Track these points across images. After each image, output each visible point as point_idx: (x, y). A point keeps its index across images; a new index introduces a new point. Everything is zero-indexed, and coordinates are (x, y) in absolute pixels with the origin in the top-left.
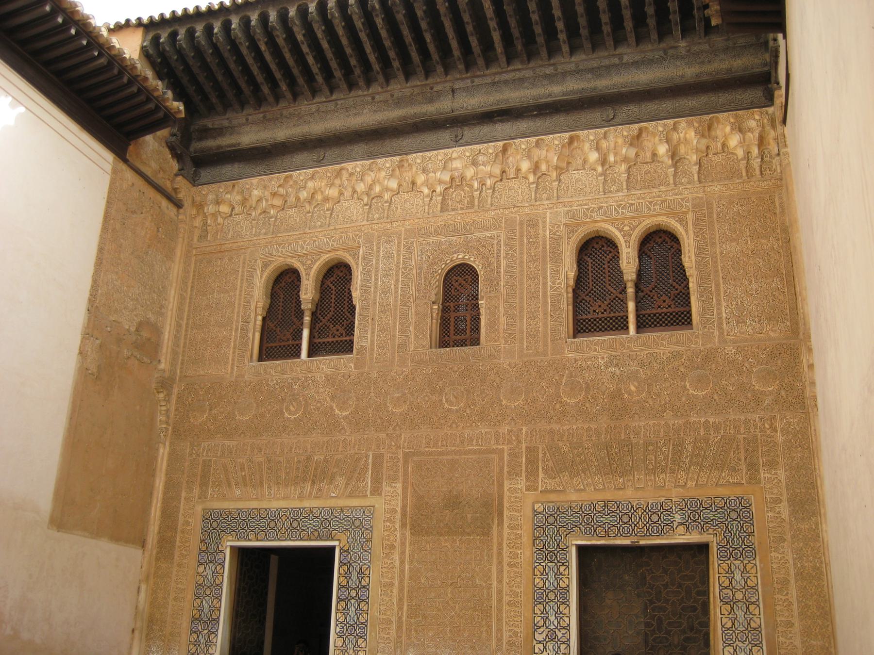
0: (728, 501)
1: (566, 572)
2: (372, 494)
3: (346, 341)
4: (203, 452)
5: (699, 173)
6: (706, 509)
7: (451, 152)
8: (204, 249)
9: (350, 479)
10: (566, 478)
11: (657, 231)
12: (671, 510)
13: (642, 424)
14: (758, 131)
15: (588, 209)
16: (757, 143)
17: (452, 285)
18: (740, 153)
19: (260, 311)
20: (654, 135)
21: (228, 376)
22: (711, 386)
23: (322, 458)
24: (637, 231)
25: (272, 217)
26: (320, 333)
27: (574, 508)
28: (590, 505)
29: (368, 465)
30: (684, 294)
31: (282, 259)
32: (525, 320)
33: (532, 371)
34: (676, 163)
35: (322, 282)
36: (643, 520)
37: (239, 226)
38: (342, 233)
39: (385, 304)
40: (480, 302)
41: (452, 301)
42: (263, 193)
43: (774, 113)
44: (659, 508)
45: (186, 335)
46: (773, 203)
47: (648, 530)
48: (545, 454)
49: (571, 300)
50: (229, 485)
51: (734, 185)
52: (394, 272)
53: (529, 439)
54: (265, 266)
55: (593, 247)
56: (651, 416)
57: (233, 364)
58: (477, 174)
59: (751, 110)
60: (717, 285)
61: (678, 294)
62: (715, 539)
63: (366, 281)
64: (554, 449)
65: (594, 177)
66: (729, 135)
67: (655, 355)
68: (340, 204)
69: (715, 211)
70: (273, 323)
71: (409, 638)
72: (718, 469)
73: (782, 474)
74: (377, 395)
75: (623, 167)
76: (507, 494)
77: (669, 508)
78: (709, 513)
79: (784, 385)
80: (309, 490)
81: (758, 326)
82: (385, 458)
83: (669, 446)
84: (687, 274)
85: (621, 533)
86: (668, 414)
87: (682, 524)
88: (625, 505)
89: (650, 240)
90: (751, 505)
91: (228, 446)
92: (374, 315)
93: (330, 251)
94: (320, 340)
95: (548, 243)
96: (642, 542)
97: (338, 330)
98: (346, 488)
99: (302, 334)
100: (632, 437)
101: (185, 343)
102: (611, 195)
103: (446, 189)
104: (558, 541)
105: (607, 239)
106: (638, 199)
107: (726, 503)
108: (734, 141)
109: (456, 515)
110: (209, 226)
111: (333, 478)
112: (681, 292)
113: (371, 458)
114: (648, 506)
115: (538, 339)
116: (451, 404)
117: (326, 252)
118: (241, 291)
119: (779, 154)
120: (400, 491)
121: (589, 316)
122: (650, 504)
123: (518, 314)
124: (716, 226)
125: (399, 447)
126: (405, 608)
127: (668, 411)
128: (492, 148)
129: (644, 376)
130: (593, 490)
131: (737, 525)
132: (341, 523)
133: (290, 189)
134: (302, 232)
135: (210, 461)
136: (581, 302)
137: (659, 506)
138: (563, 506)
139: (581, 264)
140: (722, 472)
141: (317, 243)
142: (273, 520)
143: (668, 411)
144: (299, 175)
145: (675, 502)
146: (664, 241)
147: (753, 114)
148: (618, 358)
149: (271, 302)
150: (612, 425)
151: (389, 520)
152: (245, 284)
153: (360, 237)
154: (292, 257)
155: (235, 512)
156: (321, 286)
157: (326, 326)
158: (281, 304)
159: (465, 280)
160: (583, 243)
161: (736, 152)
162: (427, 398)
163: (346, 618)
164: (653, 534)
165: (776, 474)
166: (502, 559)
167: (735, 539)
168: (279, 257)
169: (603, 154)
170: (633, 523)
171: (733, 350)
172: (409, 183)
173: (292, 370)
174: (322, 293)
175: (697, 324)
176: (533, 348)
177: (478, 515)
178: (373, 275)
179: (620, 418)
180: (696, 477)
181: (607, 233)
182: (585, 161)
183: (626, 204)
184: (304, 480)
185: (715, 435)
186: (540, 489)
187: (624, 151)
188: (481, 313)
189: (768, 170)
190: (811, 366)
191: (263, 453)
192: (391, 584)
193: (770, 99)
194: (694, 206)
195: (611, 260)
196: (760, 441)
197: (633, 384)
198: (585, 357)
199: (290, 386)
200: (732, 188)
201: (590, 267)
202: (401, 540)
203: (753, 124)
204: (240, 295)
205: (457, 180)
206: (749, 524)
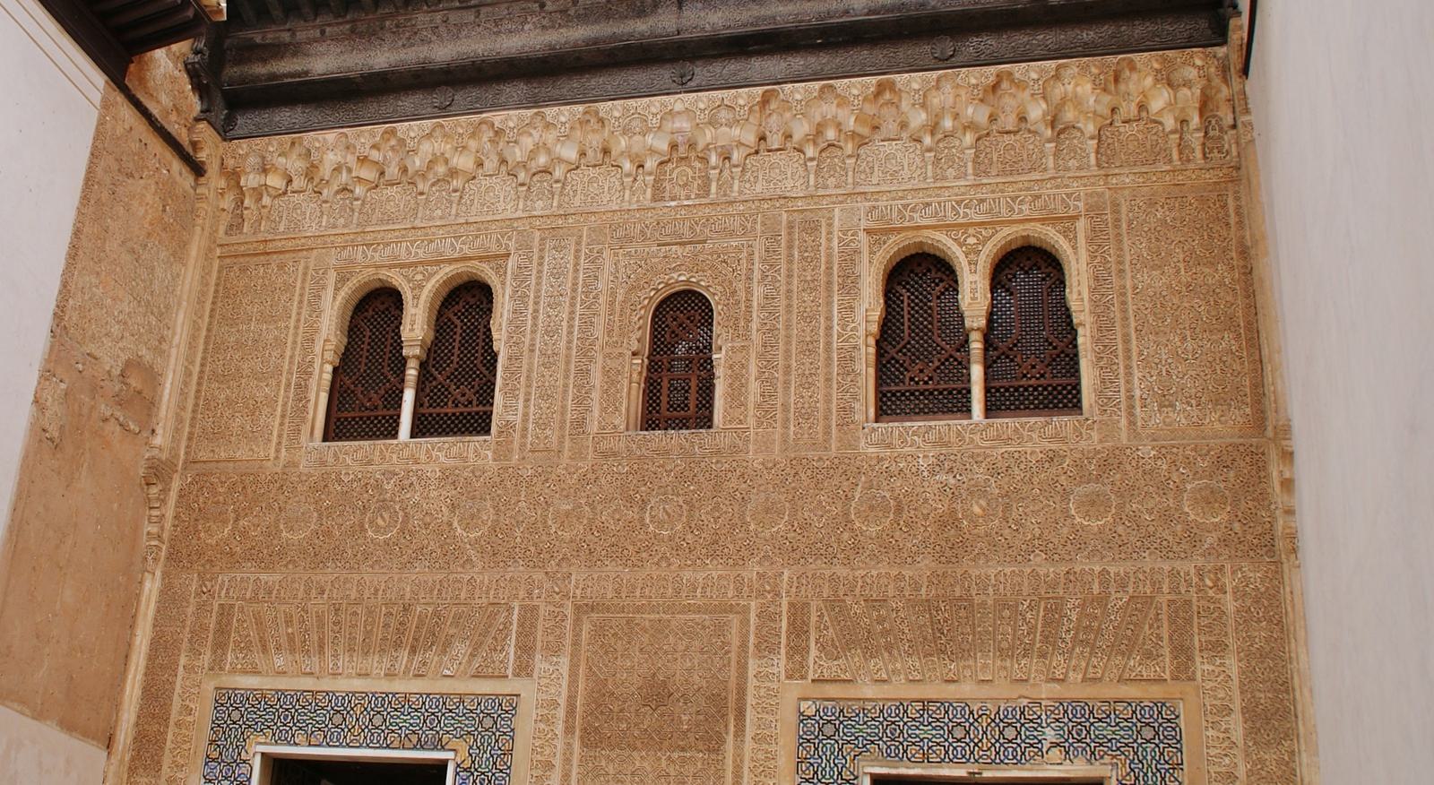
0: (1139, 708)
3: (477, 413)
5: (1097, 152)
6: (1100, 720)
7: (672, 101)
10: (856, 659)
11: (1023, 247)
12: (1039, 721)
13: (992, 572)
14: (1199, 86)
15: (905, 206)
16: (1197, 105)
17: (667, 326)
18: (1170, 122)
19: (329, 356)
20: (1020, 85)
22: (1114, 511)
24: (989, 245)
25: (357, 199)
26: (431, 398)
27: (869, 711)
28: (898, 708)
30: (1067, 355)
32: (793, 389)
33: (802, 475)
34: (1059, 134)
35: (439, 312)
36: (989, 737)
37: (299, 211)
38: (479, 230)
39: (549, 352)
40: (714, 356)
41: (665, 353)
42: (345, 158)
43: (1227, 56)
44: (1018, 717)
46: (1224, 206)
47: (998, 753)
49: (873, 357)
51: (1159, 175)
52: (567, 299)
53: (794, 589)
54: (342, 280)
55: (912, 271)
56: (1008, 559)
58: (716, 138)
59: (1188, 50)
60: (1127, 341)
61: (1058, 356)
62: (1114, 773)
64: (837, 609)
65: (918, 152)
66: (1150, 89)
67: (1016, 455)
68: (476, 181)
69: (1124, 216)
70: (350, 378)
72: (1123, 654)
73: (1233, 665)
74: (532, 506)
75: (969, 138)
76: (752, 682)
77: (1035, 716)
78: (1105, 729)
79: (1239, 514)
80: (404, 662)
83: (1039, 611)
84: (1075, 321)
85: (951, 757)
86: (1038, 559)
87: (1058, 745)
88: (959, 709)
89: (1011, 262)
90: (1177, 717)
92: (530, 371)
93: (456, 260)
94: (431, 410)
95: (836, 260)
96: (986, 774)
97: (463, 395)
99: (401, 398)
100: (974, 594)
102: (946, 184)
103: (661, 163)
104: (840, 766)
105: (935, 257)
106: (993, 192)
107: (1134, 712)
108: (1159, 101)
110: (246, 208)
112: (1062, 352)
114: (998, 713)
115: (815, 422)
116: (660, 525)
117: (451, 261)
118: (298, 321)
119: (1234, 127)
121: (902, 388)
122: (1002, 709)
123: (781, 378)
124: (1126, 243)
125: (566, 596)
127: (1037, 551)
128: (744, 96)
129: (997, 491)
130: (903, 681)
131: (1153, 750)
132: (460, 722)
133: (390, 153)
136: (889, 362)
137: (1019, 713)
138: (849, 707)
139: (890, 299)
140: (1128, 659)
141: (433, 246)
142: (339, 712)
143: (1037, 551)
145: (1046, 706)
146: (1035, 265)
147: (1192, 57)
148: (952, 457)
149: (349, 343)
150: (939, 572)
153: (510, 239)
154: (390, 267)
155: (273, 696)
156: (437, 320)
157: (443, 387)
158: (365, 347)
159: (688, 318)
160: (894, 264)
161: (1161, 119)
162: (617, 517)
164: (1006, 761)
165: (1222, 664)
167: (1150, 774)
168: (368, 267)
169: (934, 113)
170: (972, 740)
171: (1153, 453)
172: (598, 150)
174: (438, 331)
175: (1091, 406)
176: (806, 436)
177: (701, 717)
178: (531, 302)
179: (954, 560)
180: (1084, 664)
181: (939, 249)
182: (904, 125)
183: (971, 200)
185: (1118, 595)
186: (811, 676)
187: (970, 110)
188: (717, 374)
189: (1216, 151)
190: (1288, 484)
193: (1219, 35)
194: (1089, 208)
195: (943, 294)
196: (1195, 608)
197: (977, 502)
198: (896, 455)
200: (1155, 179)
201: (906, 304)
203: (1192, 73)
204: (296, 328)
205: (681, 149)
206: (1175, 750)
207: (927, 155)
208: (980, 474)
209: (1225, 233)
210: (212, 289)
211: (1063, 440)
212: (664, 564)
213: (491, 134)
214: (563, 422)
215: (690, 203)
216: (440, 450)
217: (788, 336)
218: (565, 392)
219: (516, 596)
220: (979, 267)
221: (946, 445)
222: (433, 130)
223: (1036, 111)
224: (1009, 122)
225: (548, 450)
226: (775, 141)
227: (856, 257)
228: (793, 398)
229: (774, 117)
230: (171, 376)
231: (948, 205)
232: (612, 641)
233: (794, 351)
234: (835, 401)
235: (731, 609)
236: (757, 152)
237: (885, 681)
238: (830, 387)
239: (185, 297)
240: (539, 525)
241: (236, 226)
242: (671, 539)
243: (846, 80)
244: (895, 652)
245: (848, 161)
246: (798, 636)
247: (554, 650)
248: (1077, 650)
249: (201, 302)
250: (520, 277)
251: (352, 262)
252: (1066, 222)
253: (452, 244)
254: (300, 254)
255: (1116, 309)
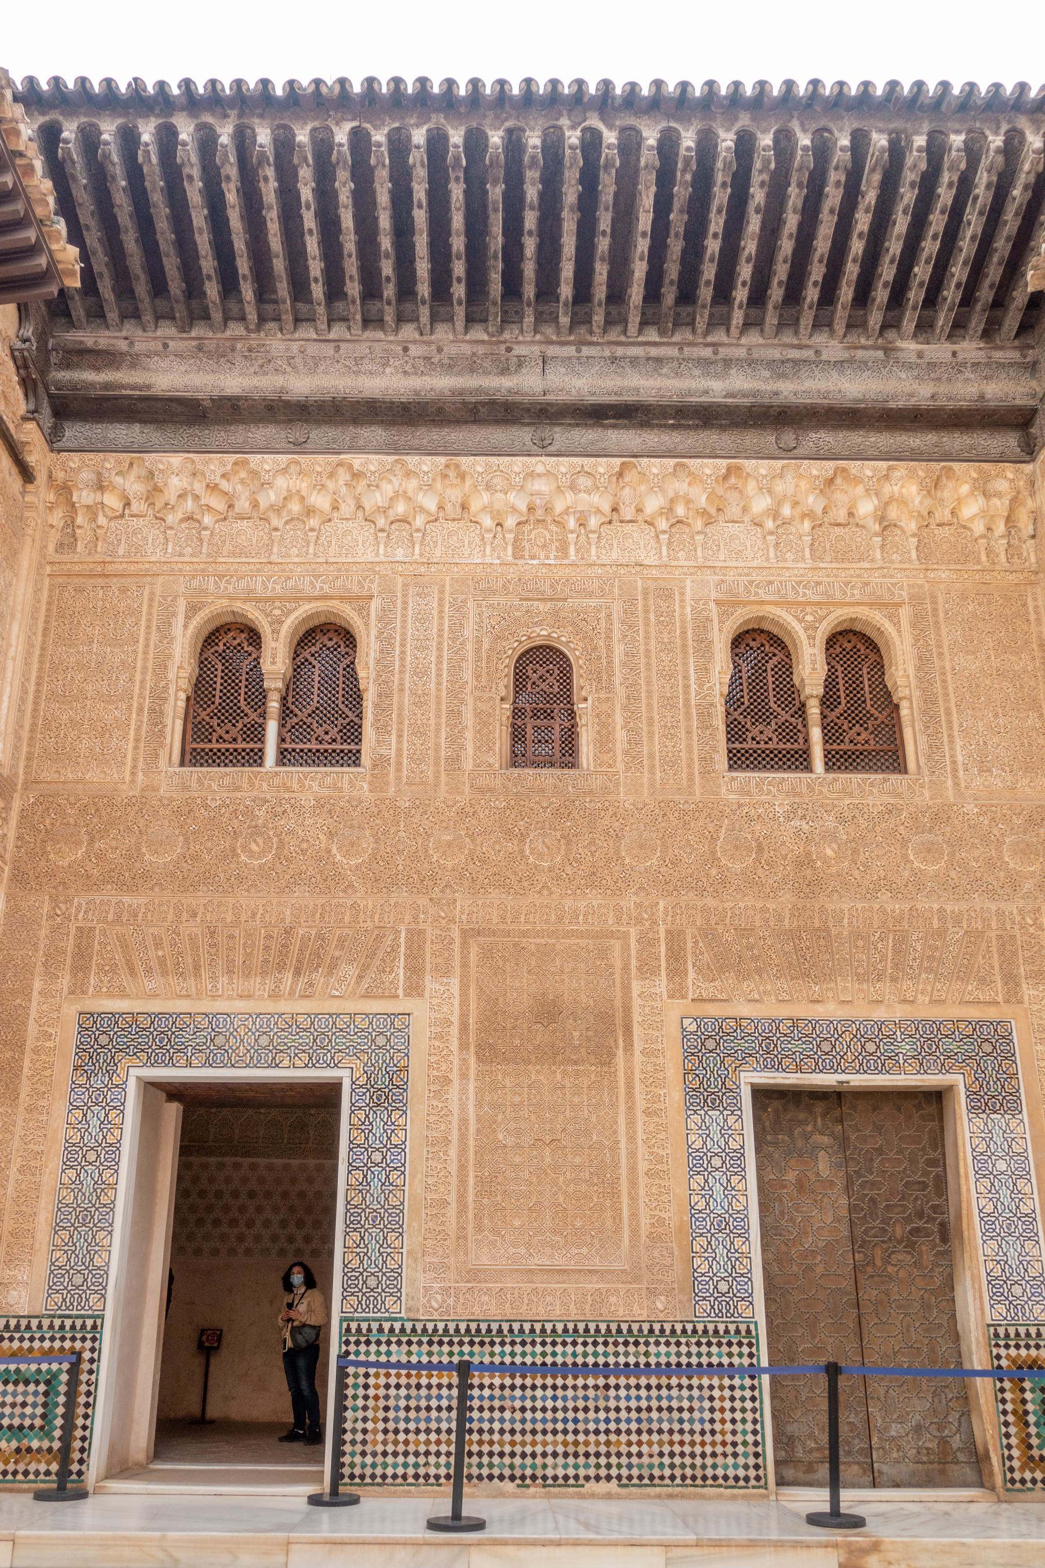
1: (737, 1126)
2: (407, 994)
4: (78, 911)
6: (947, 1036)
8: (69, 566)
9: (365, 968)
14: (1009, 497)
15: (751, 582)
18: (979, 528)
19: (184, 684)
20: (857, 480)
21: (125, 787)
23: (313, 933)
24: (825, 623)
25: (205, 529)
29: (399, 946)
31: (225, 602)
32: (656, 739)
45: (35, 710)
46: (1024, 605)
48: (696, 943)
50: (132, 971)
53: (669, 918)
54: (193, 609)
57: (134, 767)
60: (948, 713)
63: (385, 652)
66: (967, 496)
68: (332, 524)
71: (479, 1229)
72: (962, 980)
75: (807, 525)
76: (636, 1002)
81: (1009, 778)
82: (429, 936)
91: (130, 906)
92: (401, 708)
93: (317, 598)
98: (358, 983)
101: (34, 725)
106: (828, 576)
109: (554, 1031)
110: (79, 527)
111: (333, 967)
113: (403, 935)
116: (540, 856)
117: (310, 599)
118: (147, 646)
119: (1033, 537)
120: (456, 990)
124: (944, 630)
125: (453, 921)
126: (471, 1181)
128: (603, 466)
129: (845, 837)
134: (265, 560)
135: (92, 929)
141: (291, 583)
144: (266, 463)
151: (439, 1036)
152: (154, 637)
153: (372, 581)
162: (497, 847)
163: (364, 1199)
166: (633, 1103)
168: (220, 598)
173: (252, 785)
178: (397, 644)
184: (281, 967)
186: (690, 996)
187: (811, 499)
191: (198, 919)
192: (447, 1141)
194: (912, 597)
199: (249, 812)
202: (461, 1069)
204: (146, 653)
207: (769, 538)
208: (830, 821)
209: (1026, 628)
210: (44, 607)
211: (899, 795)
212: (545, 893)
213: (348, 477)
214: (437, 759)
215: (552, 562)
216: (313, 779)
217: (649, 692)
218: (438, 730)
219: (402, 920)
220: (817, 642)
221: (800, 795)
222: (288, 466)
223: (866, 508)
224: (841, 516)
225: (423, 783)
226: (628, 513)
227: (708, 624)
228: (657, 747)
229: (627, 490)
230: (8, 689)
231: (789, 585)
232: (500, 963)
233: (655, 705)
234: (696, 751)
235: (612, 935)
236: (610, 522)
237: (756, 1001)
238: (691, 739)
239: (19, 608)
240: (420, 853)
241: (68, 542)
242: (551, 869)
243: (699, 460)
244: (765, 975)
245: (697, 537)
246: (676, 959)
247: (445, 972)
248: (924, 976)
249: (35, 619)
250: (384, 617)
251: (204, 592)
252: (891, 608)
253: (311, 583)
254: (144, 580)
255: (938, 685)
